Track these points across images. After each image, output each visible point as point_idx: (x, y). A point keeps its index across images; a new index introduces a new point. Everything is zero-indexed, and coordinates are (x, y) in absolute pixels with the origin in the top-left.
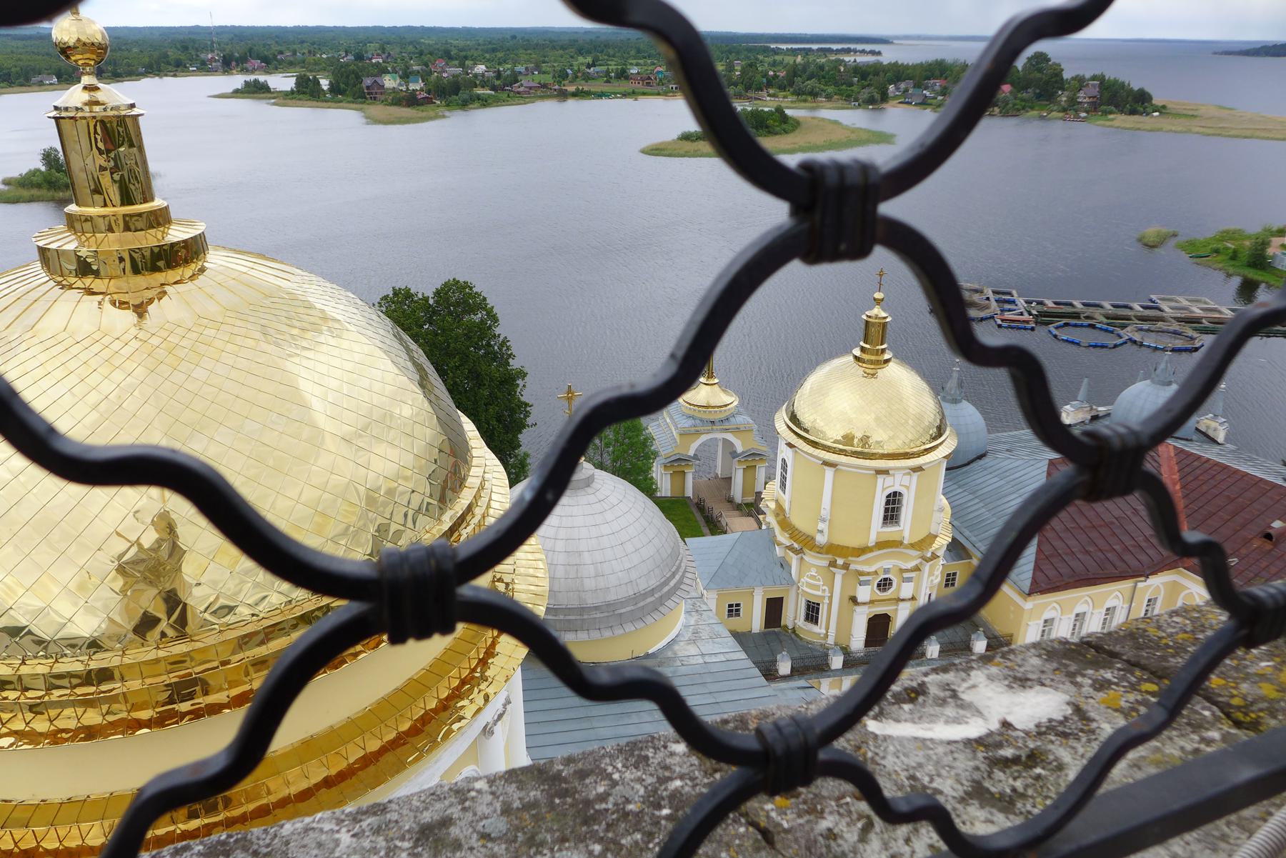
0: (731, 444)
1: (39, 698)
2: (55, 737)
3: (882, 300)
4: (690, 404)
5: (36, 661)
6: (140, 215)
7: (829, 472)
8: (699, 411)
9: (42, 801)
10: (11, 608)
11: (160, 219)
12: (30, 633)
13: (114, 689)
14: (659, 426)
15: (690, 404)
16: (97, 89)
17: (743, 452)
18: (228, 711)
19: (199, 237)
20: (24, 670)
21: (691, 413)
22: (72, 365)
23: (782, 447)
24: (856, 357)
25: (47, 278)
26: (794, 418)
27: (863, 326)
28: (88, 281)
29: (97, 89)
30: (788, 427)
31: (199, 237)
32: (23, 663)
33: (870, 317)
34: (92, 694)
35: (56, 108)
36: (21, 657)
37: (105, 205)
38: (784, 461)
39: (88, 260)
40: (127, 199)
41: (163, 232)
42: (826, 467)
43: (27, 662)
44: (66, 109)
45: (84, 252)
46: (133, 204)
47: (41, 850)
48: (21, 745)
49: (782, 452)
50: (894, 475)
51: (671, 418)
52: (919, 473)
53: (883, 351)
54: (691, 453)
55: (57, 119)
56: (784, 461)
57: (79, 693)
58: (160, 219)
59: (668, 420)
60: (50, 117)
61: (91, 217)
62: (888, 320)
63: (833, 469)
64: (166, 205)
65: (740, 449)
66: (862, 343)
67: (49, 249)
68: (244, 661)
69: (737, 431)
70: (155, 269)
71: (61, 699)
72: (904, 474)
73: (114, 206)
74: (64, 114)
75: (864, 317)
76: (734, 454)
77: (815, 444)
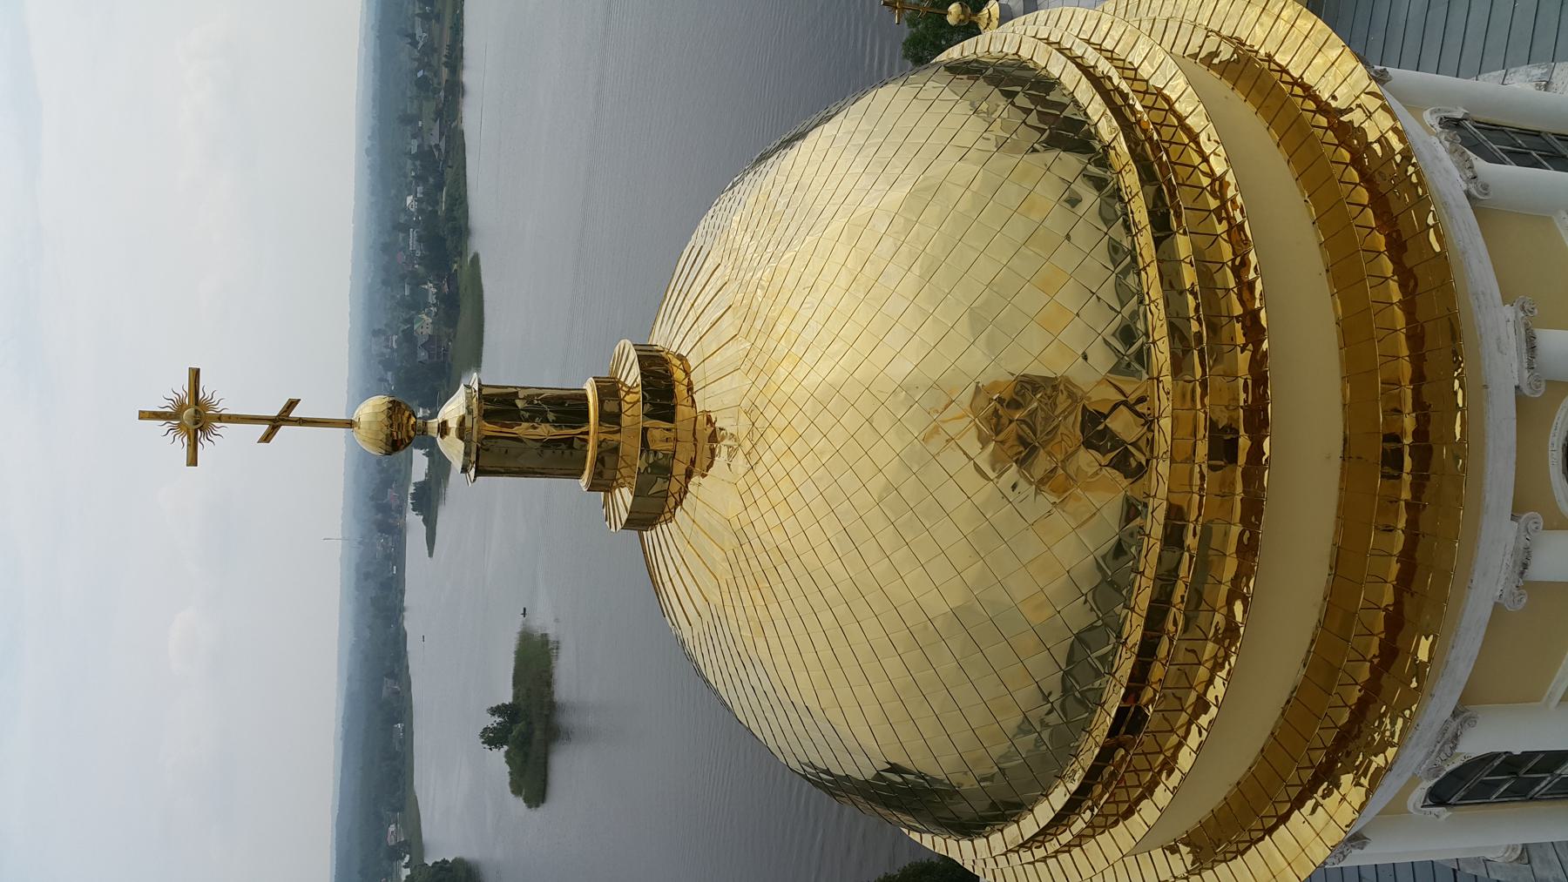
1: (1191, 557)
2: (1248, 549)
5: (1143, 560)
6: (601, 402)
9: (1325, 599)
10: (1068, 572)
11: (609, 389)
12: (1104, 557)
13: (1201, 472)
16: (444, 423)
18: (1265, 346)
19: (639, 353)
20: (1150, 572)
22: (775, 495)
25: (664, 526)
28: (679, 469)
29: (444, 423)
31: (639, 353)
32: (1142, 573)
34: (1201, 497)
35: (465, 470)
36: (1133, 575)
37: (586, 441)
39: (651, 461)
40: (584, 416)
41: (628, 393)
43: (1141, 570)
44: (467, 454)
45: (640, 464)
46: (587, 399)
47: (1391, 609)
48: (1248, 587)
55: (479, 473)
57: (1197, 513)
58: (609, 389)
60: (474, 480)
61: (598, 454)
64: (591, 379)
67: (631, 507)
68: (1202, 316)
70: (669, 392)
71: (1198, 537)
73: (587, 433)
74: (473, 458)
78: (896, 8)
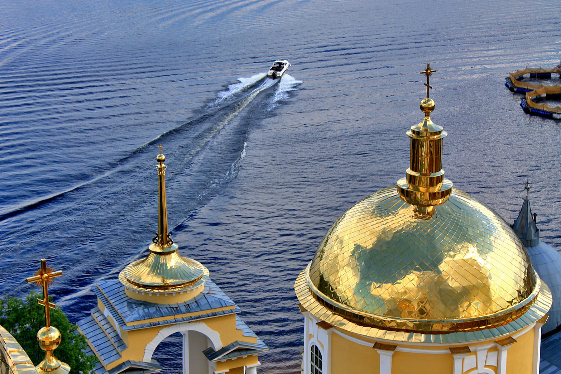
0: (205, 338)
3: (432, 109)
4: (135, 284)
7: (385, 357)
8: (155, 294)
14: (93, 322)
15: (139, 286)
17: (223, 350)
21: (142, 298)
23: (310, 327)
24: (402, 191)
26: (323, 285)
27: (409, 149)
30: (318, 299)
33: (418, 133)
38: (315, 350)
42: (379, 351)
49: (311, 336)
50: (475, 353)
51: (112, 309)
52: (509, 347)
53: (440, 179)
54: (148, 358)
56: (315, 350)
59: (107, 312)
62: (445, 134)
63: (391, 353)
65: (218, 345)
66: (409, 171)
69: (212, 318)
72: (490, 350)
75: (409, 133)
76: (211, 354)
77: (359, 320)
78: (42, 275)
